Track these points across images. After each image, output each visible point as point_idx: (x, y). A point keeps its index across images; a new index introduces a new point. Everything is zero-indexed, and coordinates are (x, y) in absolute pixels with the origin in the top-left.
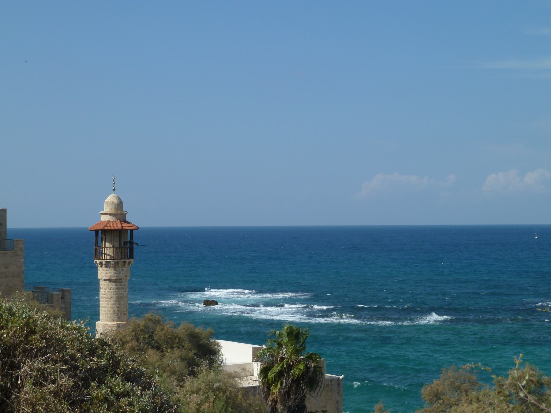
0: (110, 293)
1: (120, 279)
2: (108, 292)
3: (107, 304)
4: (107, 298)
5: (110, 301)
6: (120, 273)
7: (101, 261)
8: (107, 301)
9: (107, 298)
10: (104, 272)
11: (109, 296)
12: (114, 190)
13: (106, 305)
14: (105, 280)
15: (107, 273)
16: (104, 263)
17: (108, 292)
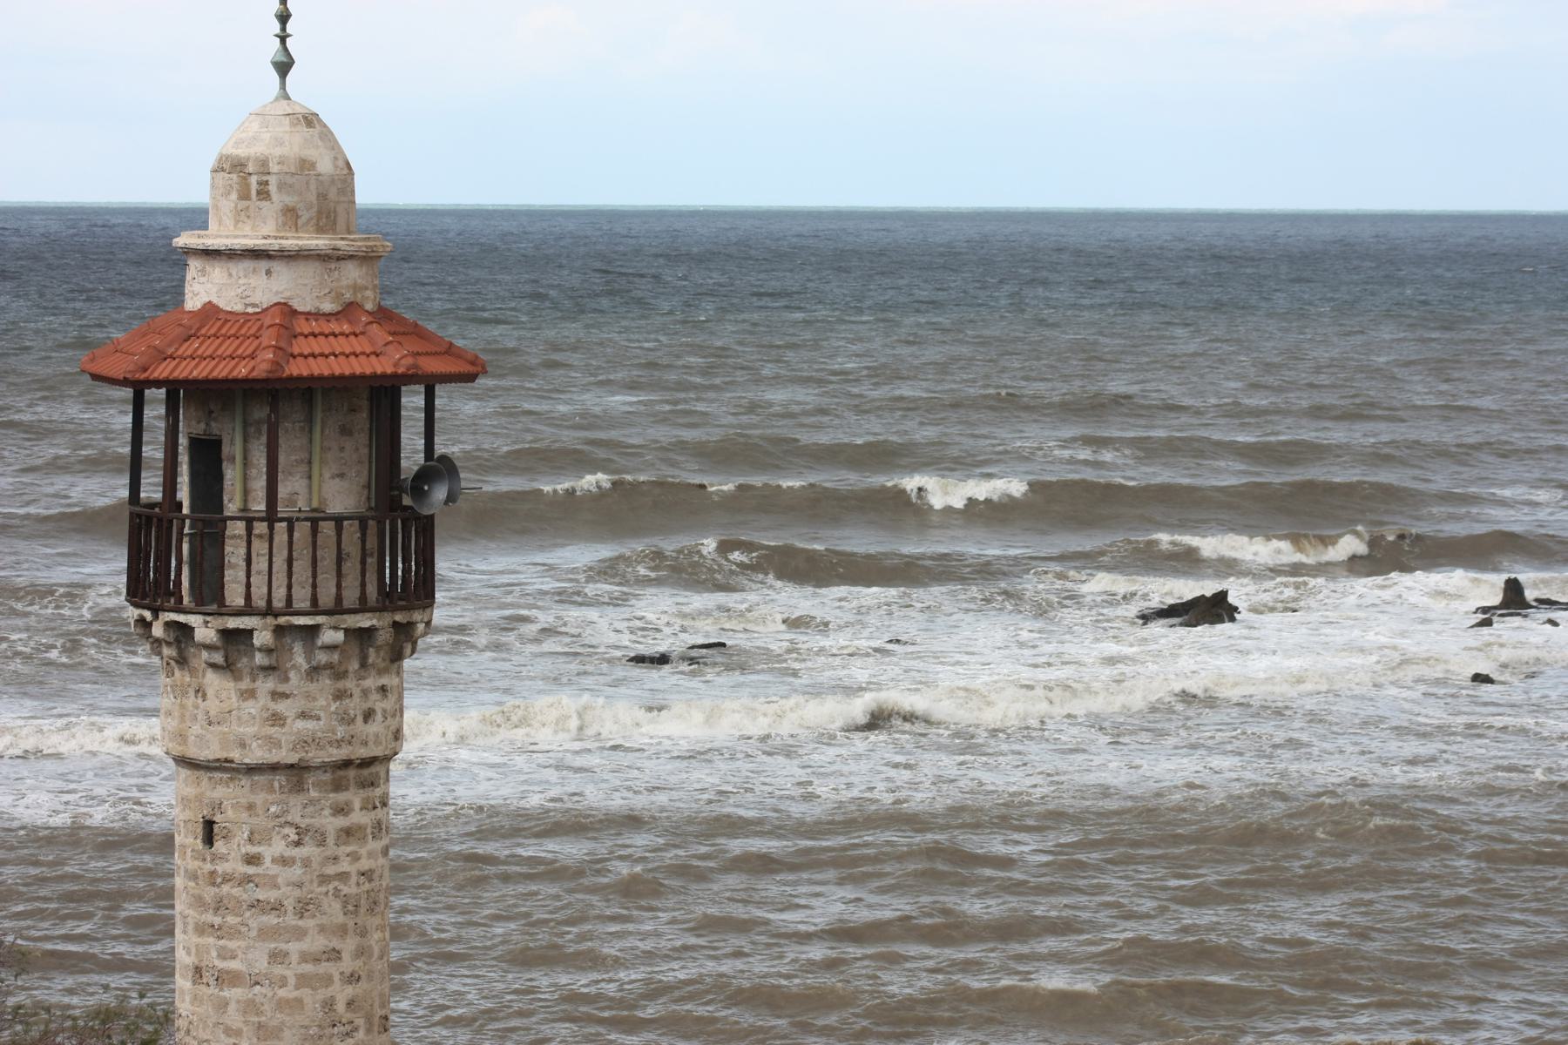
0: (297, 872)
1: (367, 763)
2: (284, 861)
3: (277, 957)
4: (277, 907)
5: (300, 934)
6: (368, 715)
7: (233, 623)
8: (265, 934)
9: (277, 907)
10: (252, 707)
11: (289, 896)
12: (284, 67)
13: (262, 964)
14: (251, 770)
15: (277, 719)
16: (262, 638)
17: (284, 861)
